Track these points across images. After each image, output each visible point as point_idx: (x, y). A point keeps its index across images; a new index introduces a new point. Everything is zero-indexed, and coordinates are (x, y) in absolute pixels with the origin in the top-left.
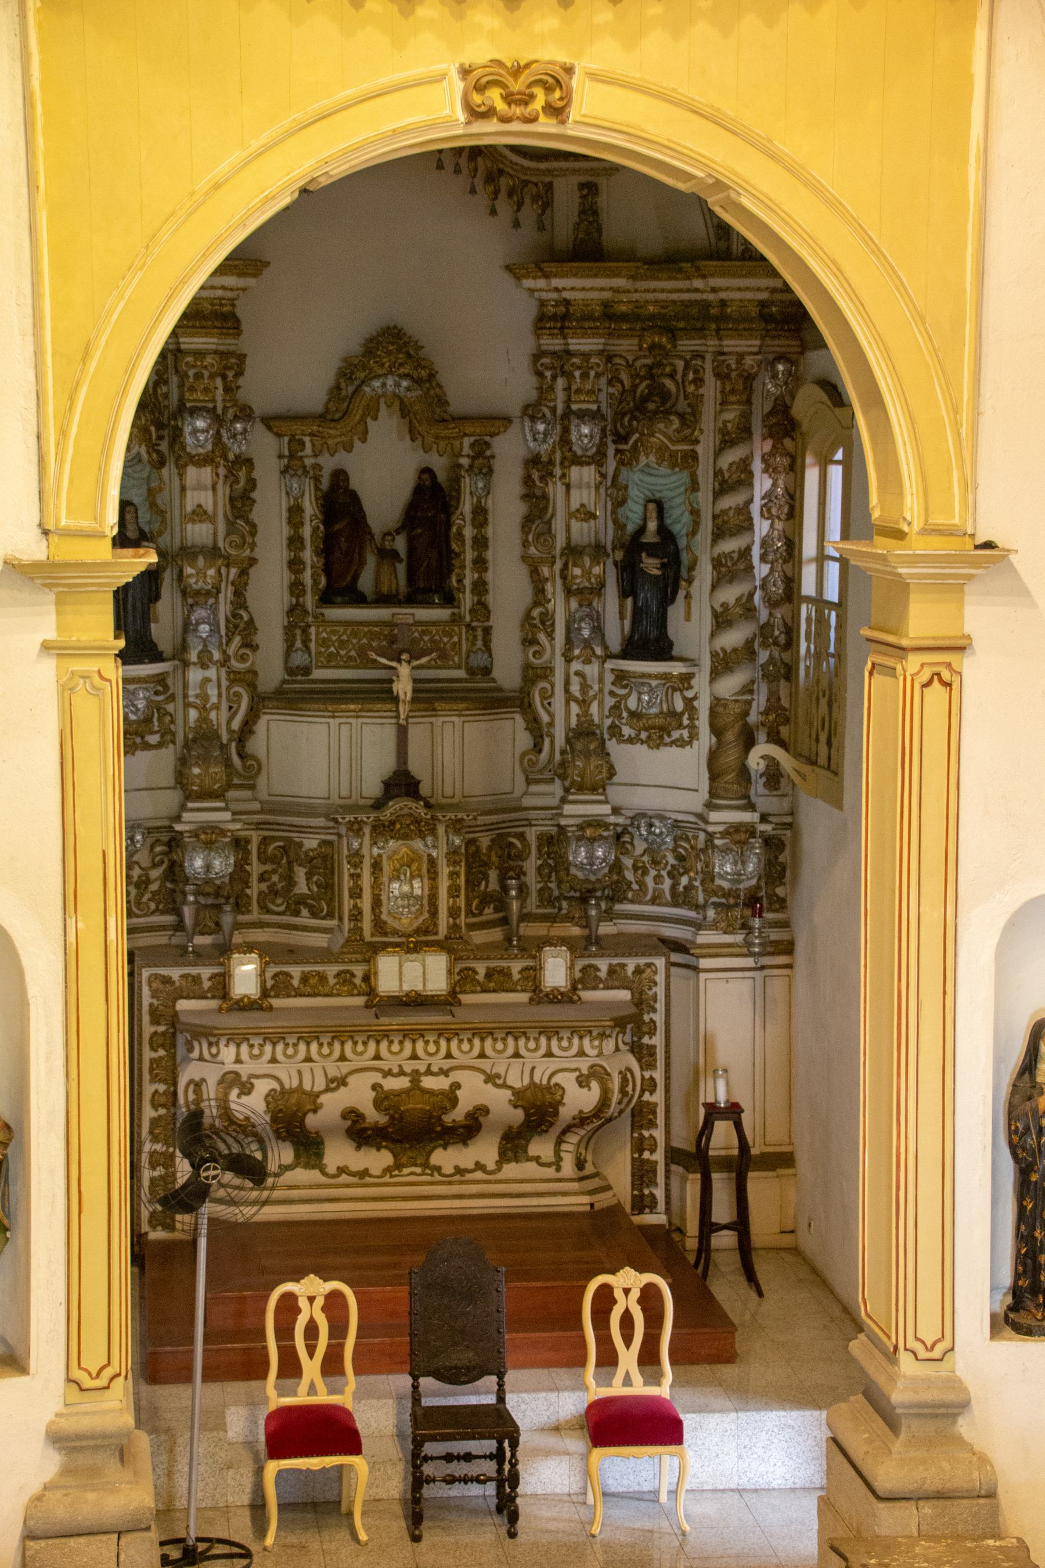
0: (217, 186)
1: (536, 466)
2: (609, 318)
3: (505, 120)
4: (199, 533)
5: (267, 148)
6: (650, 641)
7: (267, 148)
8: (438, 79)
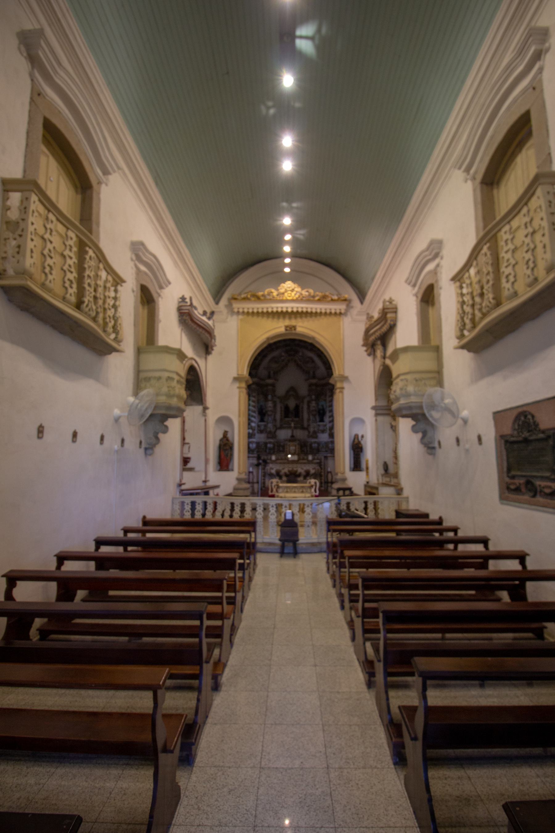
1: (309, 402)
2: (316, 385)
4: (270, 409)
6: (322, 420)
8: (281, 327)
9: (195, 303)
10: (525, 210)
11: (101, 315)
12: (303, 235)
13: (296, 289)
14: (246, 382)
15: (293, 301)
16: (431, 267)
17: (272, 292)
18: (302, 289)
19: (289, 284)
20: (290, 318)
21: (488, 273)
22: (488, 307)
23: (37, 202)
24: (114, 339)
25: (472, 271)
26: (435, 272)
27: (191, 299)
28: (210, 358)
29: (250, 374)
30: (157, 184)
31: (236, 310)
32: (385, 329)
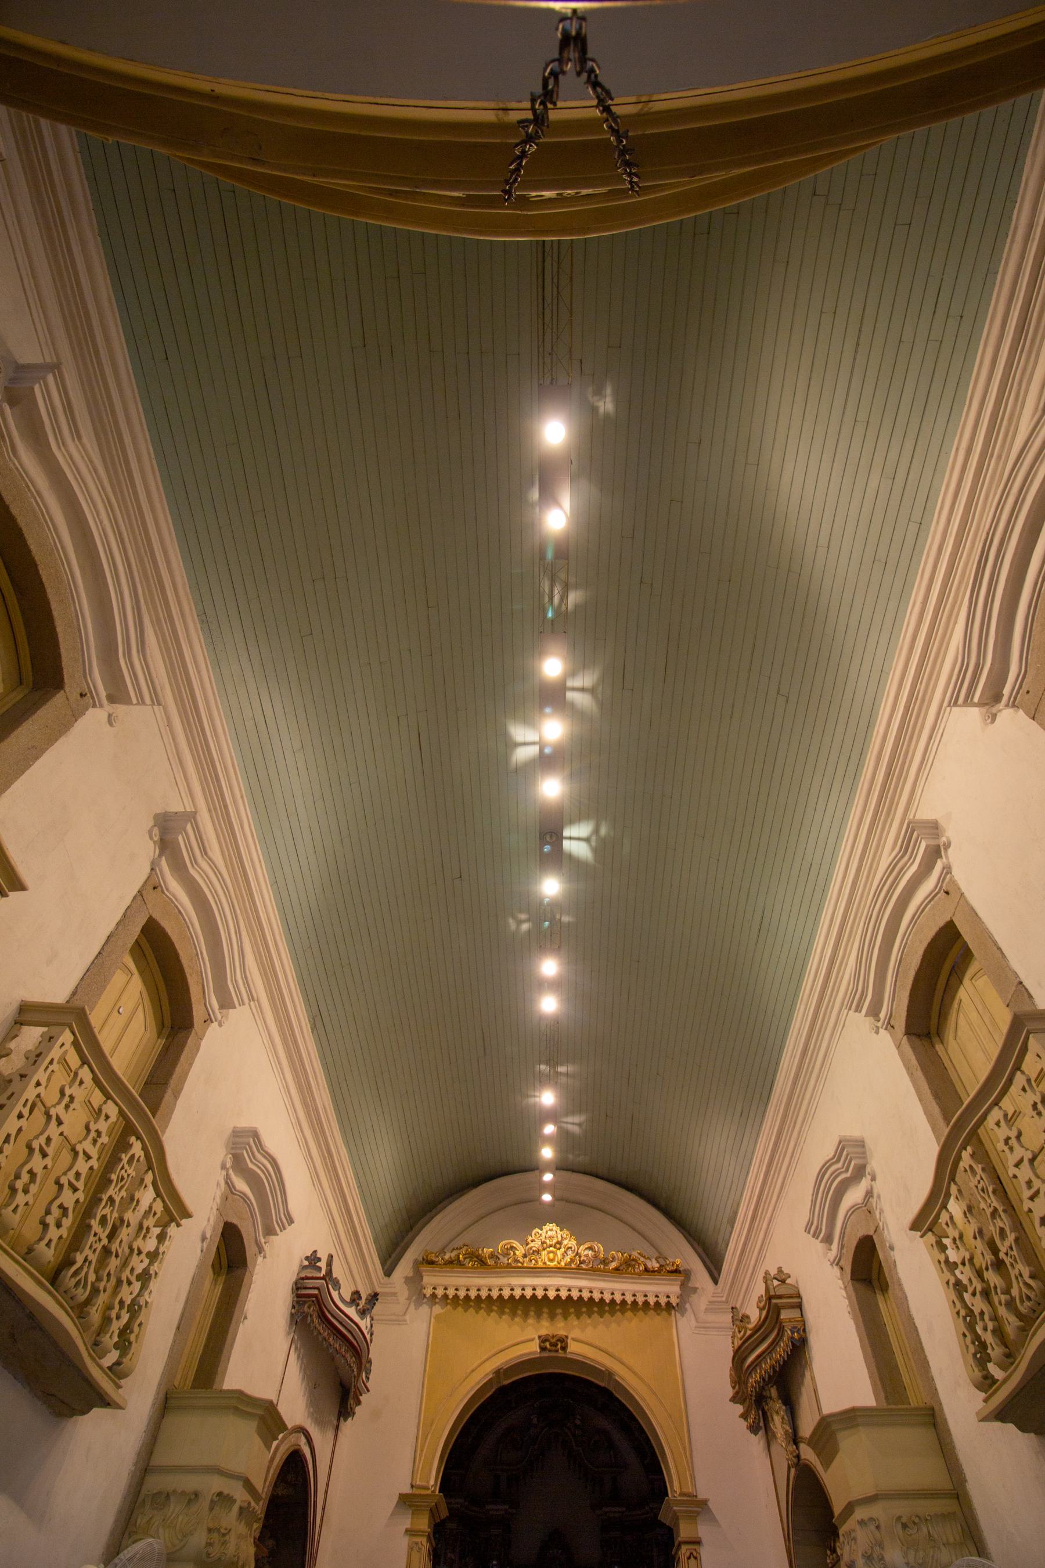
0: (473, 1371)
3: (550, 1351)
5: (487, 1359)
7: (487, 1359)
8: (533, 1340)
9: (337, 1272)
10: (1019, 1079)
11: (102, 1299)
12: (580, 1125)
13: (565, 1242)
14: (433, 1512)
15: (559, 1270)
16: (854, 1196)
17: (512, 1248)
18: (579, 1244)
19: (551, 1231)
20: (552, 1317)
21: (995, 1213)
22: (1029, 1298)
23: (68, 1046)
24: (110, 1368)
25: (955, 1207)
26: (867, 1207)
27: (331, 1257)
28: (348, 1427)
29: (447, 1484)
30: (314, 1027)
31: (428, 1292)
32: (781, 1351)
